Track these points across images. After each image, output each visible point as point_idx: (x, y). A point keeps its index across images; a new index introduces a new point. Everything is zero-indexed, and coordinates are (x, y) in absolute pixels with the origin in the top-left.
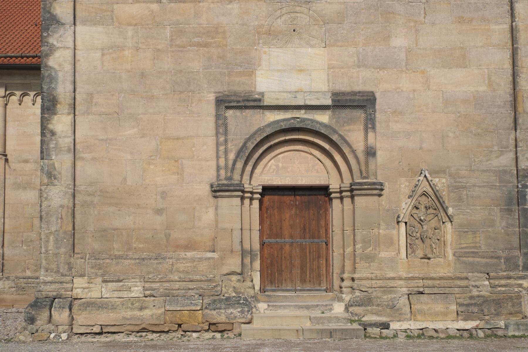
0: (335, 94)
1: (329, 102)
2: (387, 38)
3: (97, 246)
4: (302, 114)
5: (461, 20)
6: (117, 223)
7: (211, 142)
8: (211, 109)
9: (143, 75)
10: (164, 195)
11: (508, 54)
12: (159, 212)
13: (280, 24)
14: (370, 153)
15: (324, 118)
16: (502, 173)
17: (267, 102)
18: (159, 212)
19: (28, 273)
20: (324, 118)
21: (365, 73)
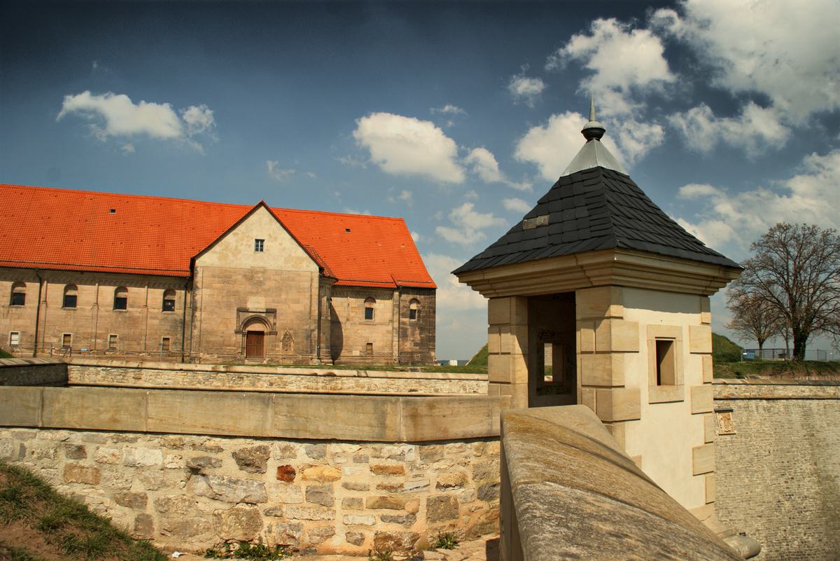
0: (267, 309)
1: (265, 311)
2: (280, 296)
3: (206, 345)
4: (258, 314)
5: (298, 292)
6: (211, 339)
7: (235, 320)
8: (236, 311)
9: (219, 302)
10: (223, 333)
11: (309, 301)
12: (222, 337)
13: (254, 291)
14: (275, 324)
15: (264, 315)
16: (306, 330)
17: (250, 310)
18: (222, 337)
19: (155, 351)
20: (264, 315)
21: (275, 304)
